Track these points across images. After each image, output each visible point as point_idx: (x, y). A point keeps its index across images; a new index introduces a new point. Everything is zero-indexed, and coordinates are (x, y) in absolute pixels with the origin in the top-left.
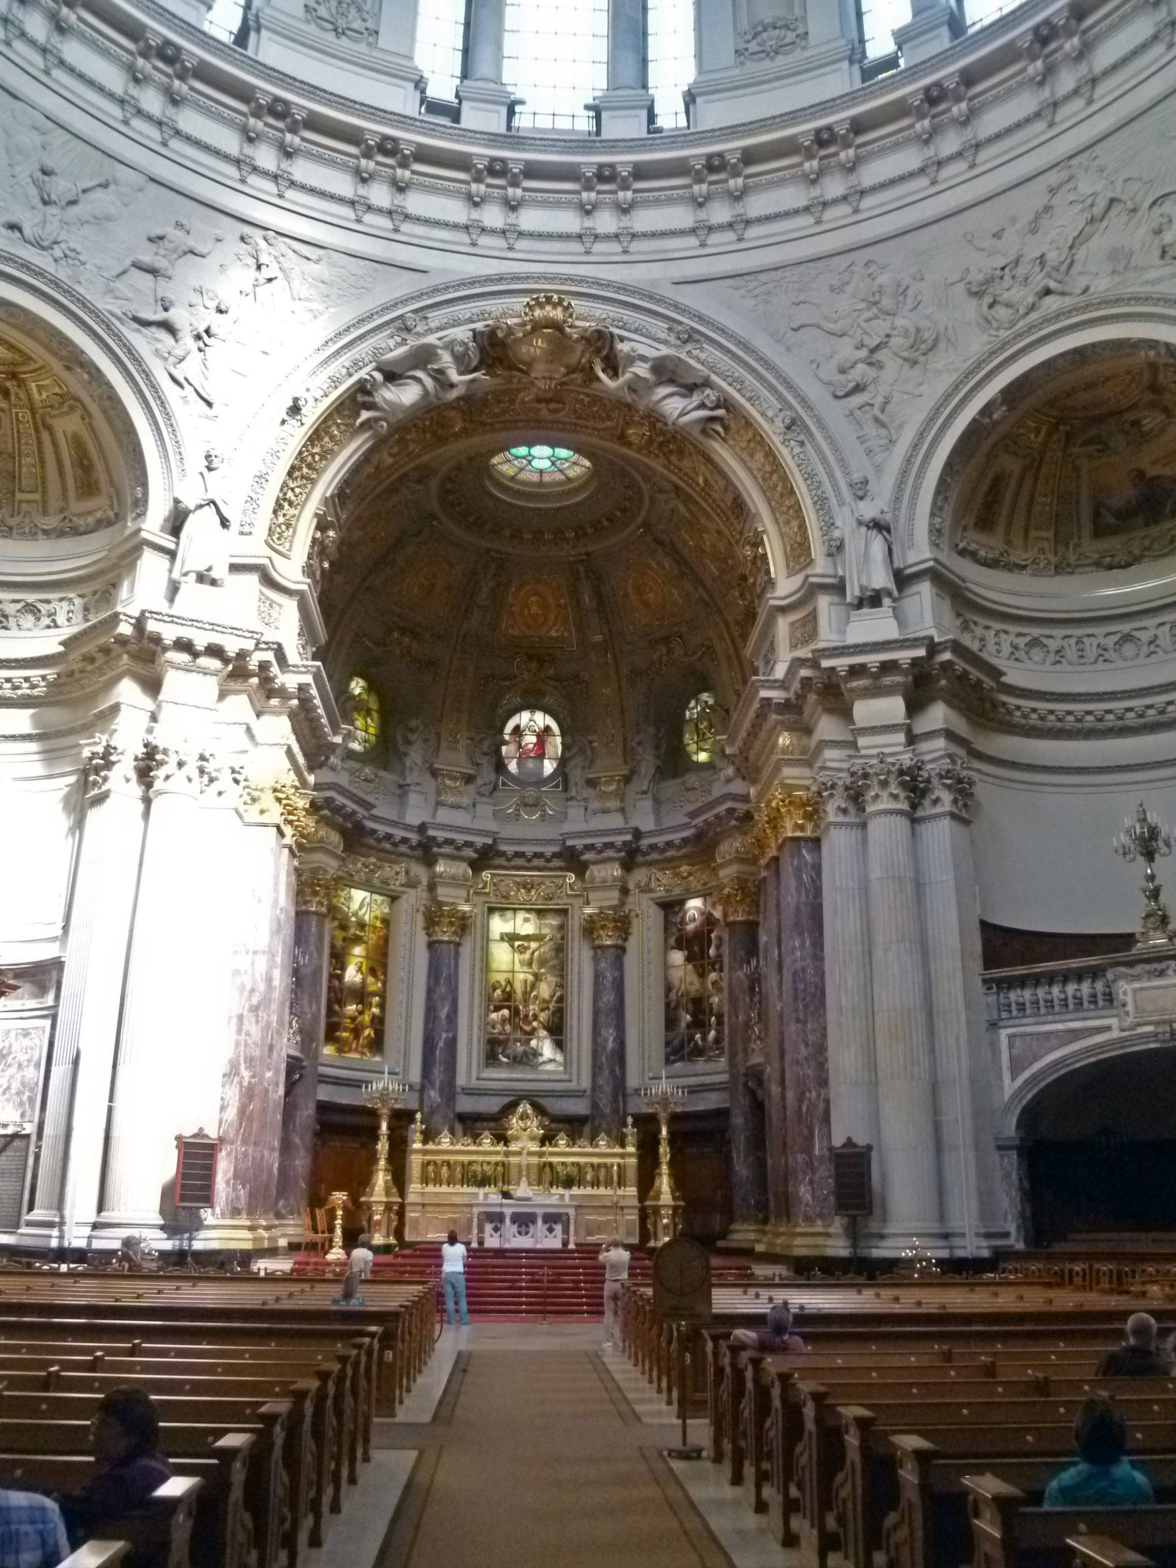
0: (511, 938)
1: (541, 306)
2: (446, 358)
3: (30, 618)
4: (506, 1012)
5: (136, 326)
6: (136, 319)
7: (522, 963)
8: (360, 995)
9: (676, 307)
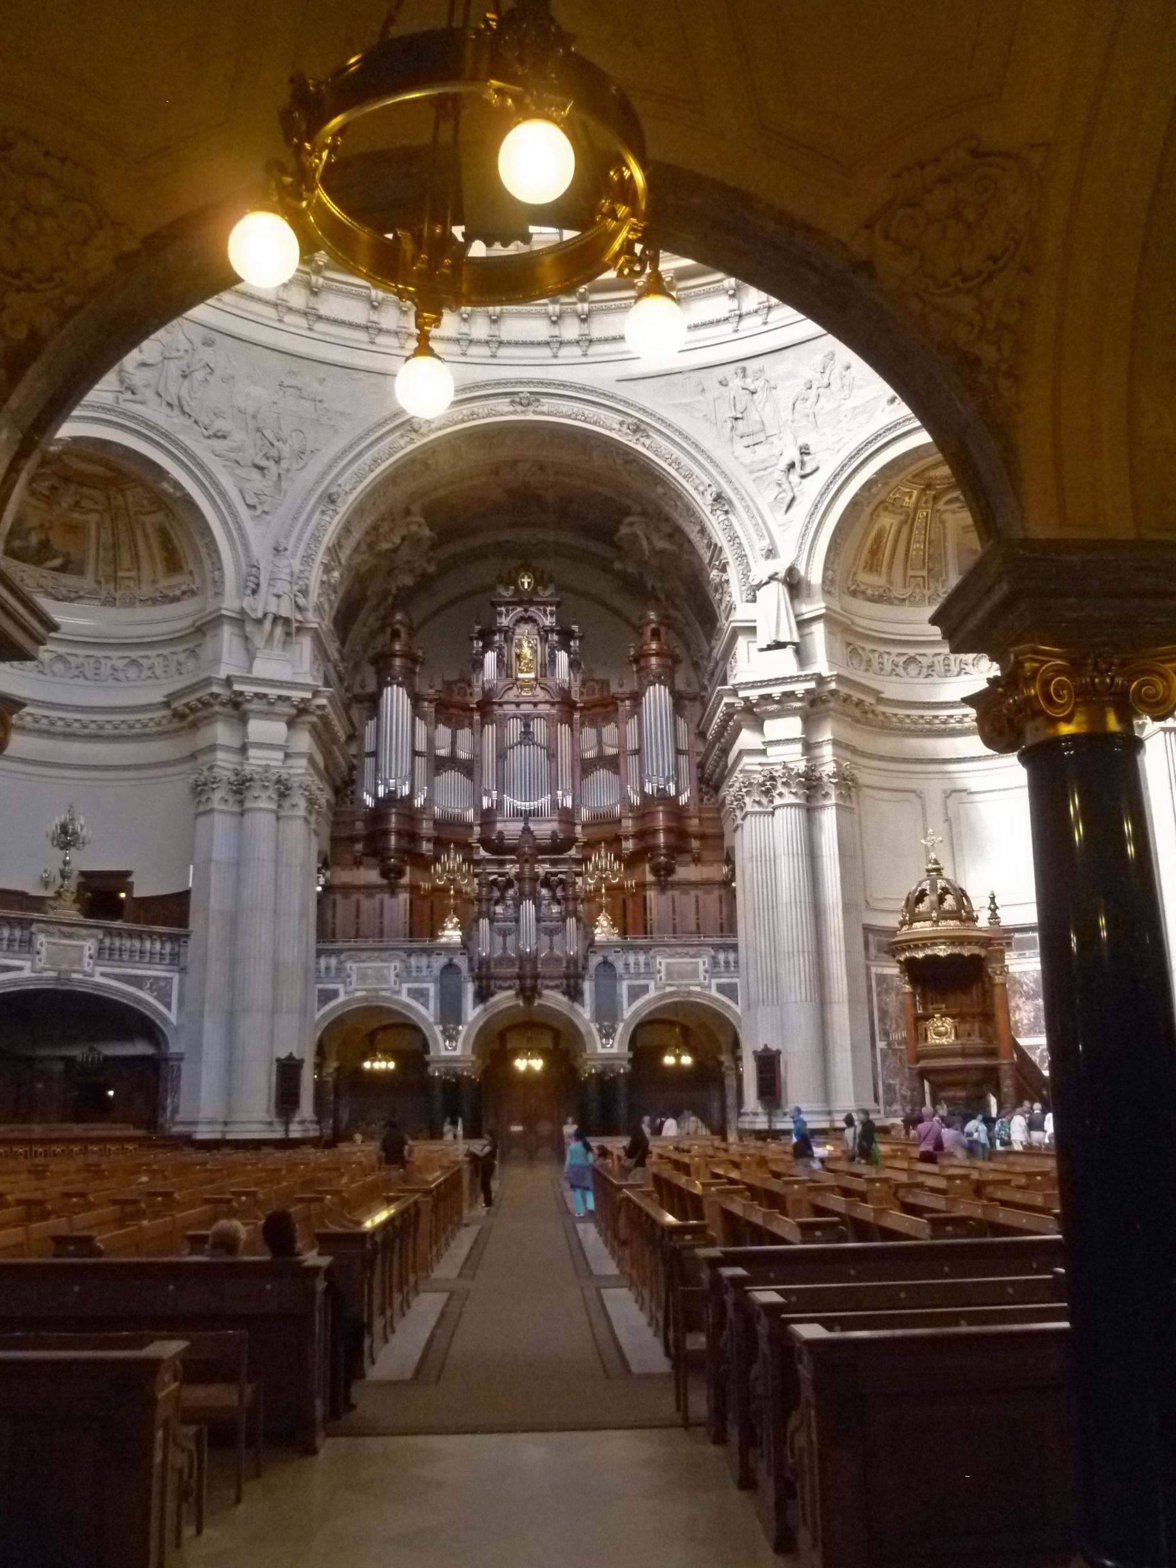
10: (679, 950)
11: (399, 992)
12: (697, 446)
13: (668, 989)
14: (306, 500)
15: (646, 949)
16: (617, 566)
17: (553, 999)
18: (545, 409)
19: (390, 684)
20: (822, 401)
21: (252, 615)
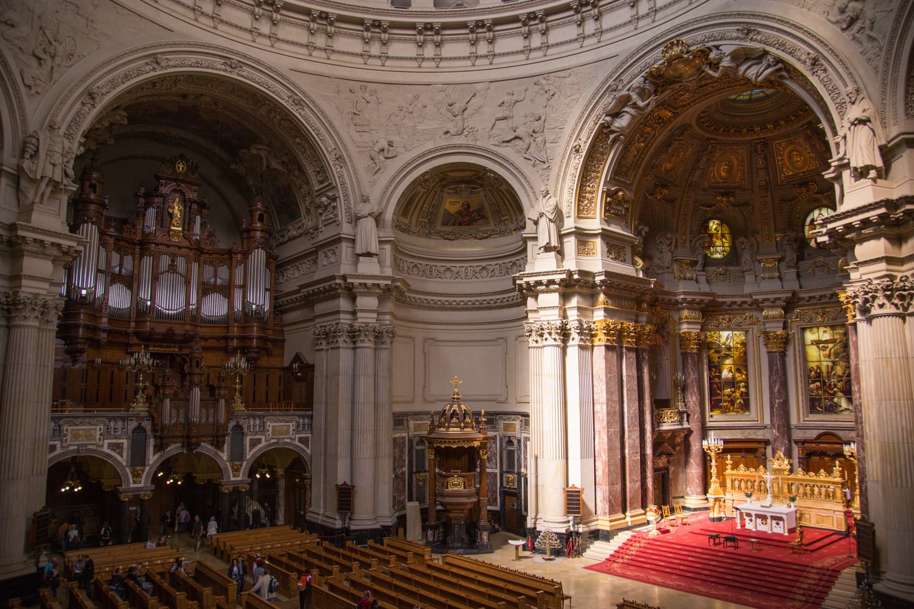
0: (817, 343)
1: (671, 48)
2: (634, 97)
3: (515, 267)
4: (818, 384)
5: (505, 144)
6: (504, 142)
7: (825, 356)
8: (732, 383)
9: (739, 15)
10: (280, 418)
11: (102, 446)
12: (330, 123)
13: (272, 441)
14: (71, 92)
15: (261, 417)
16: (233, 166)
17: (206, 448)
18: (245, 74)
19: (87, 223)
20: (406, 120)
21: (31, 175)
